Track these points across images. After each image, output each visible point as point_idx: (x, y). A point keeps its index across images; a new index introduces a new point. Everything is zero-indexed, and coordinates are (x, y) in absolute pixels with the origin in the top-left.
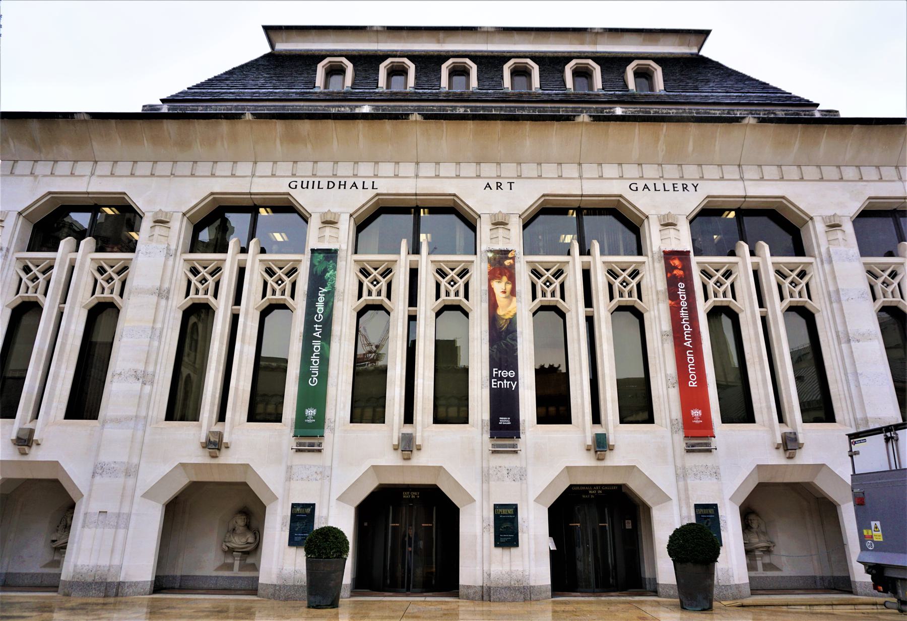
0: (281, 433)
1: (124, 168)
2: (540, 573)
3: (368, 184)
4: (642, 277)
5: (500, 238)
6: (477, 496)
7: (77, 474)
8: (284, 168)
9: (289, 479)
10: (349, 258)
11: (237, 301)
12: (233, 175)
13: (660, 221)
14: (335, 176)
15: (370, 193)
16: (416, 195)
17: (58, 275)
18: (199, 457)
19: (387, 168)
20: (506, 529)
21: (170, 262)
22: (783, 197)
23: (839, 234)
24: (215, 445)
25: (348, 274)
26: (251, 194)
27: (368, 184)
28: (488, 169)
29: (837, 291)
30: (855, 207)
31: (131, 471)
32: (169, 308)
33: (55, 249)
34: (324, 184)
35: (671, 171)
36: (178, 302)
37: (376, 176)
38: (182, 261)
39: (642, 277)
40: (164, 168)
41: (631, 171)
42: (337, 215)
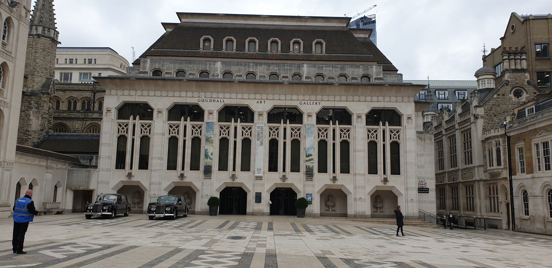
0: (199, 174)
1: (145, 93)
2: (267, 210)
3: (222, 101)
6: (251, 191)
7: (145, 184)
8: (196, 94)
9: (203, 185)
11: (185, 136)
12: (180, 96)
14: (212, 97)
15: (223, 104)
17: (130, 128)
18: (177, 180)
19: (227, 95)
20: (258, 198)
23: (360, 120)
24: (182, 176)
27: (222, 101)
28: (258, 96)
30: (367, 110)
31: (160, 184)
33: (129, 119)
34: (208, 100)
35: (313, 97)
36: (167, 136)
37: (224, 98)
40: (158, 93)
41: (301, 97)
42: (213, 111)
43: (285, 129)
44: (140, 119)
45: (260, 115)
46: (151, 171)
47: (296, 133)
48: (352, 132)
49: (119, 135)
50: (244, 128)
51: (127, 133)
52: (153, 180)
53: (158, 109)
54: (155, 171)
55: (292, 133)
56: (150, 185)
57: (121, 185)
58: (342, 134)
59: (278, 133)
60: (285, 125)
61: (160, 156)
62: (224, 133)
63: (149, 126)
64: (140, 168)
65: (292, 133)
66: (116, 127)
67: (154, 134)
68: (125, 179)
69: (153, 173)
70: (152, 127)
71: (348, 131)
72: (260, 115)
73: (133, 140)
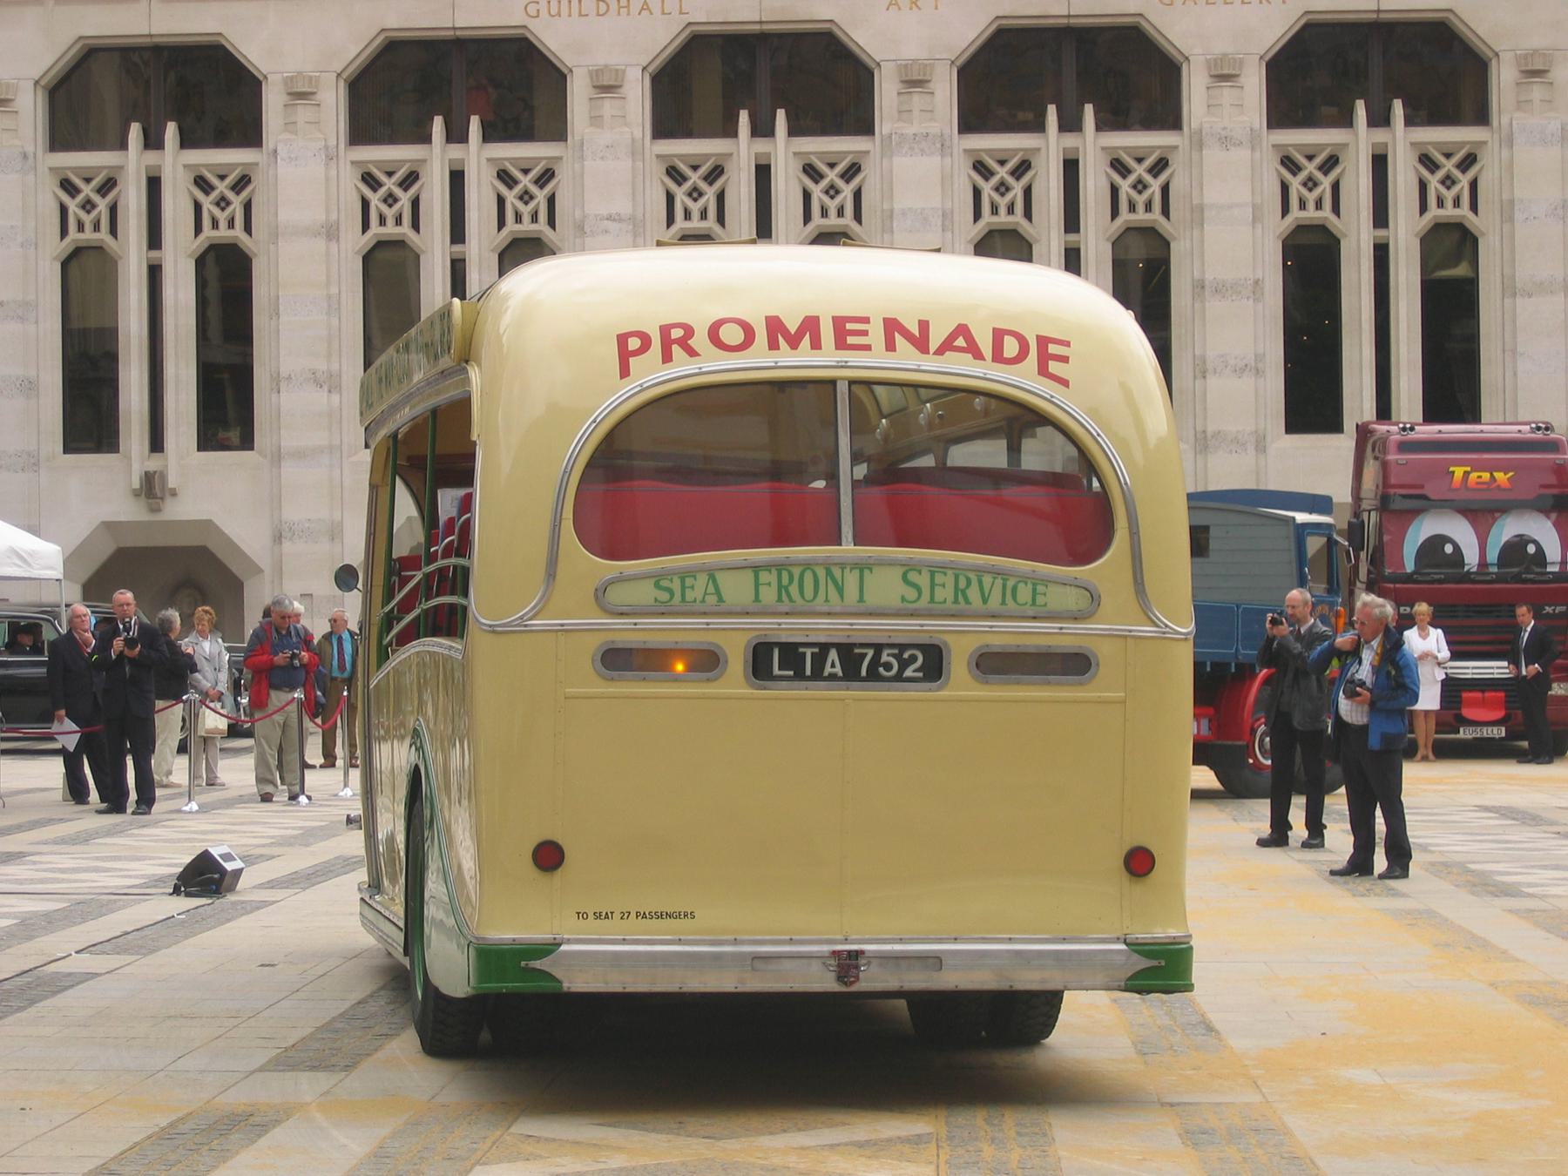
4: (1171, 175)
5: (916, 113)
10: (647, 151)
13: (1209, 68)
16: (761, 22)
21: (333, 173)
22: (1450, 10)
25: (648, 183)
26: (454, 28)
29: (1512, 202)
32: (343, 255)
36: (355, 242)
38: (349, 166)
39: (1171, 175)
42: (620, 73)
43: (1071, 168)
44: (186, 142)
45: (915, 82)
46: (277, 458)
47: (1140, 186)
48: (1489, 171)
49: (66, 246)
50: (811, 172)
51: (113, 231)
52: (293, 513)
53: (289, 81)
54: (301, 455)
55: (1114, 190)
56: (278, 538)
57: (106, 549)
58: (1434, 182)
59: (1028, 192)
60: (1070, 140)
61: (321, 366)
62: (695, 208)
63: (242, 183)
64: (207, 441)
65: (1114, 190)
66: (48, 197)
67: (275, 236)
68: (127, 510)
69: (289, 470)
70: (259, 191)
71: (1468, 161)
72: (915, 82)
73: (155, 272)
